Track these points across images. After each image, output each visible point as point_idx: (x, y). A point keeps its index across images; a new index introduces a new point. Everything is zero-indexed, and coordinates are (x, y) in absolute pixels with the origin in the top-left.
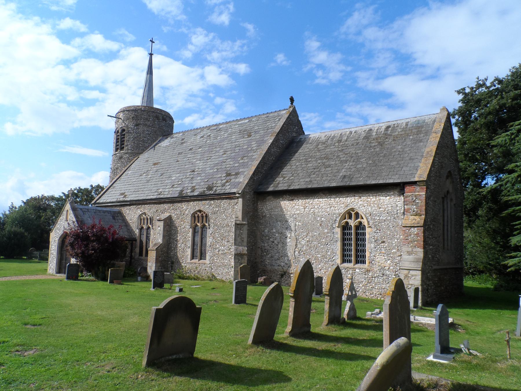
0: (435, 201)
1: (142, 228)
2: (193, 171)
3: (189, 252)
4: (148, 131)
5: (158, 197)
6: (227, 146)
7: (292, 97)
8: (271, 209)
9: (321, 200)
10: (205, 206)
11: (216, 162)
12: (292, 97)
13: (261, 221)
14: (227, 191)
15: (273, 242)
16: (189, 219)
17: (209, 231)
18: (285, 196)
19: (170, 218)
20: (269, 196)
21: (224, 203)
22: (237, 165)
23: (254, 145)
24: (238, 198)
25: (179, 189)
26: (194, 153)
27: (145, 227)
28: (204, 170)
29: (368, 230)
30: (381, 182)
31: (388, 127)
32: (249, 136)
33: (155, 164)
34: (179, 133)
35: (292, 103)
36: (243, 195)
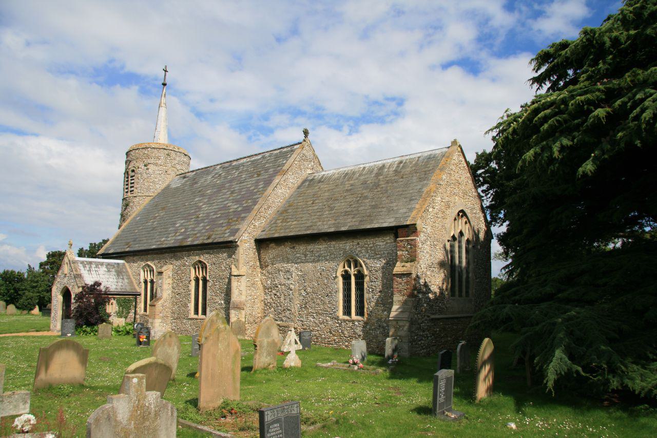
0: (435, 245)
3: (192, 306)
4: (158, 170)
5: (160, 246)
9: (320, 247)
11: (222, 206)
14: (226, 240)
15: (275, 295)
17: (209, 284)
18: (286, 243)
20: (271, 243)
22: (240, 209)
23: (261, 185)
25: (180, 237)
26: (203, 195)
27: (149, 279)
28: (208, 215)
29: (367, 279)
30: (376, 226)
31: (401, 162)
32: (259, 175)
33: (163, 209)
34: (193, 171)
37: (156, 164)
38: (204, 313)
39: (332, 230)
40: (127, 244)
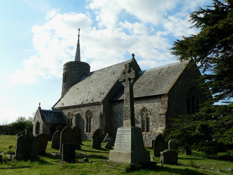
1: (69, 119)
2: (89, 92)
4: (76, 73)
6: (105, 79)
7: (133, 54)
8: (117, 109)
10: (91, 109)
12: (133, 54)
13: (114, 114)
16: (85, 114)
17: (92, 120)
19: (78, 114)
21: (97, 107)
24: (101, 104)
25: (82, 101)
30: (153, 94)
31: (169, 67)
35: (133, 57)
36: (103, 102)
37: (75, 70)
38: (90, 132)
39: (138, 97)
40: (63, 104)
